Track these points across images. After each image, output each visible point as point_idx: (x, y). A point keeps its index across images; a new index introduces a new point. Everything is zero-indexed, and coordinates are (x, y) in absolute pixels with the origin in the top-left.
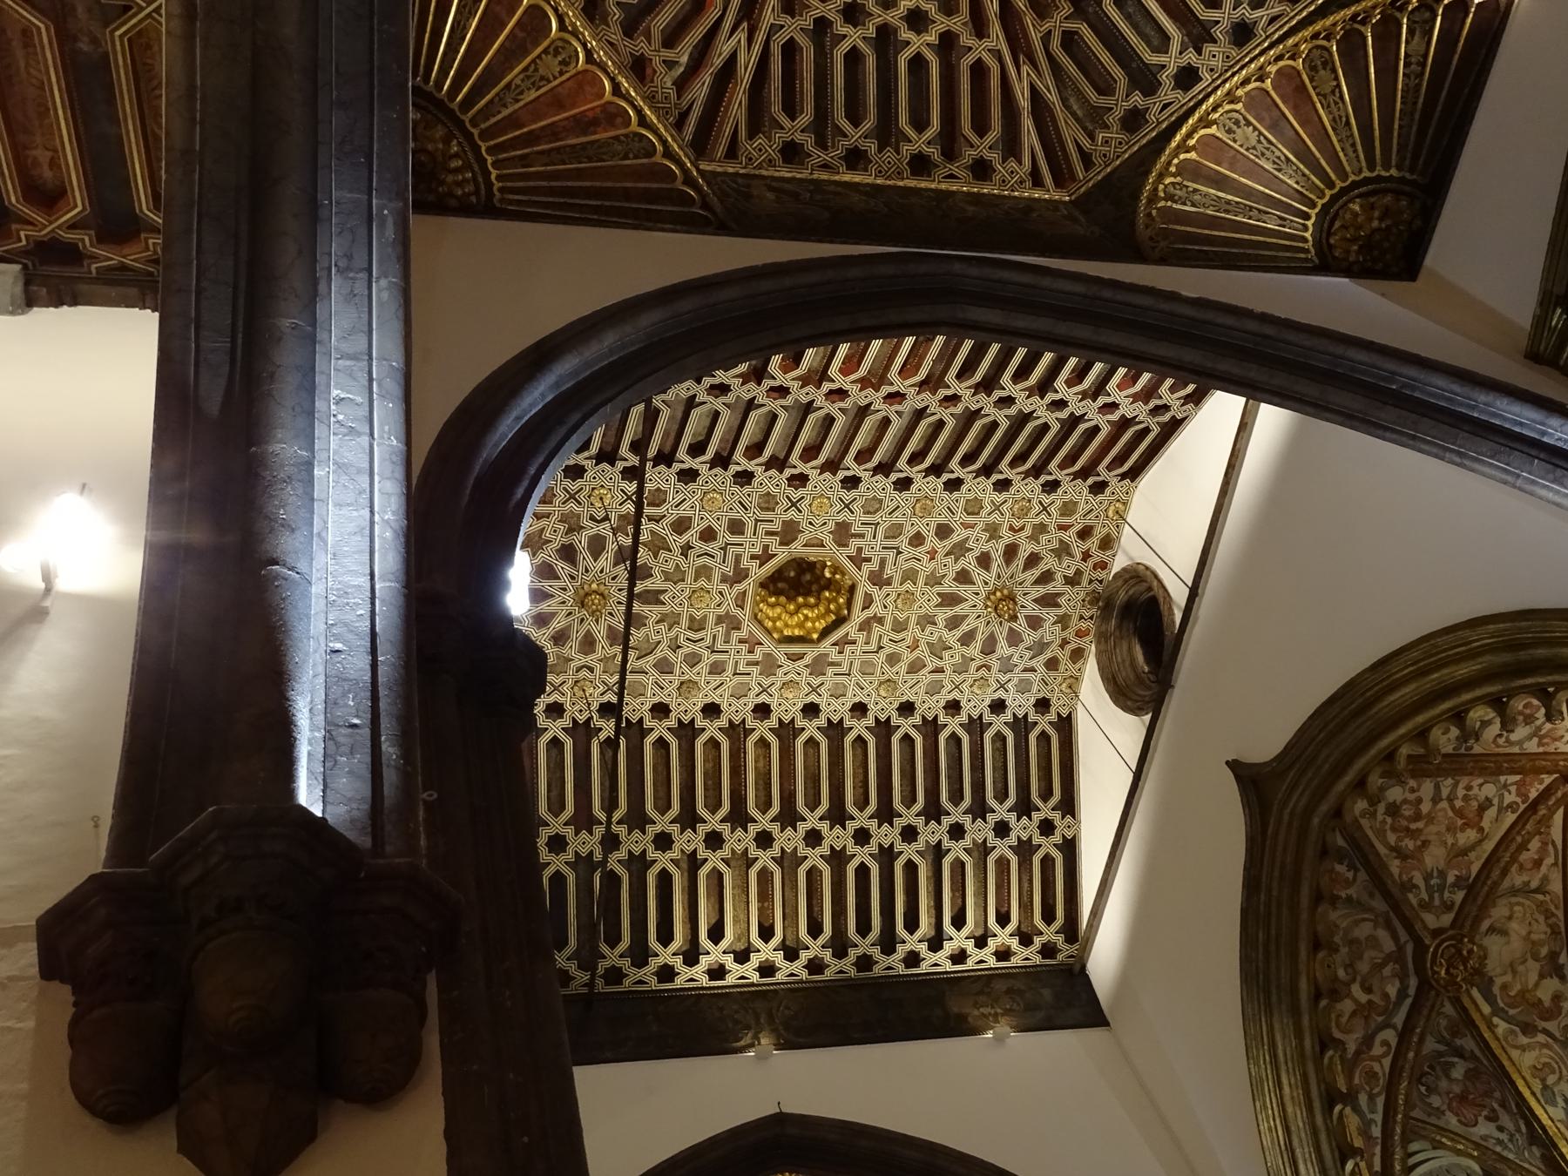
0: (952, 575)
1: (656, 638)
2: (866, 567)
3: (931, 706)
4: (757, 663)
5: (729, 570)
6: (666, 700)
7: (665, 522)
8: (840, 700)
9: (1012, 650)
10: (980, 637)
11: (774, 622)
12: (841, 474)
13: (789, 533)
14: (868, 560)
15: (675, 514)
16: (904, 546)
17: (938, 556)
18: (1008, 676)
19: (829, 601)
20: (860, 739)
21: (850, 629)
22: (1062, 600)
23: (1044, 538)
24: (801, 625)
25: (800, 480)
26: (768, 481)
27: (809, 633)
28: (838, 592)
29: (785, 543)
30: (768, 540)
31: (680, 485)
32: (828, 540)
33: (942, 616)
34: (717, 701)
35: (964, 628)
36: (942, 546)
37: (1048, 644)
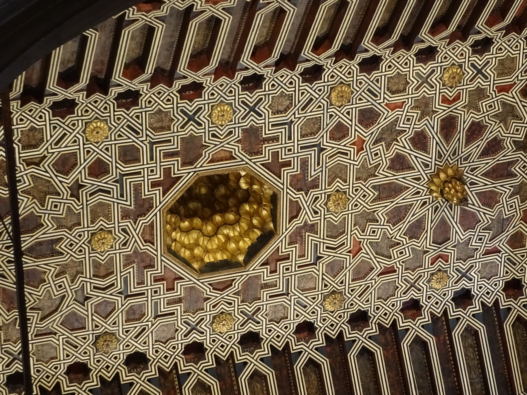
0: (386, 163)
1: (57, 293)
2: (286, 172)
3: (386, 312)
4: (180, 301)
5: (129, 203)
6: (83, 359)
7: (46, 164)
8: (282, 324)
9: (468, 233)
10: (429, 226)
11: (191, 250)
12: (239, 76)
13: (191, 151)
14: (288, 164)
15: (56, 152)
16: (326, 142)
17: (367, 146)
18: (468, 263)
19: (251, 216)
20: (312, 363)
21: (280, 243)
22: (516, 169)
23: (484, 104)
24: (222, 248)
25: (194, 90)
26: (157, 98)
27: (233, 255)
28: (260, 204)
29: (188, 162)
30: (168, 163)
31: (56, 120)
32: (237, 150)
33: (382, 209)
34: (141, 349)
35: (410, 219)
36: (369, 134)
37: (509, 219)
